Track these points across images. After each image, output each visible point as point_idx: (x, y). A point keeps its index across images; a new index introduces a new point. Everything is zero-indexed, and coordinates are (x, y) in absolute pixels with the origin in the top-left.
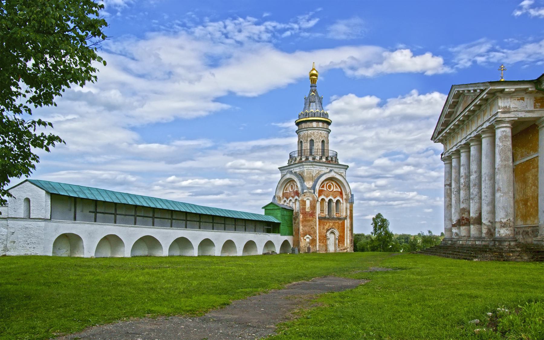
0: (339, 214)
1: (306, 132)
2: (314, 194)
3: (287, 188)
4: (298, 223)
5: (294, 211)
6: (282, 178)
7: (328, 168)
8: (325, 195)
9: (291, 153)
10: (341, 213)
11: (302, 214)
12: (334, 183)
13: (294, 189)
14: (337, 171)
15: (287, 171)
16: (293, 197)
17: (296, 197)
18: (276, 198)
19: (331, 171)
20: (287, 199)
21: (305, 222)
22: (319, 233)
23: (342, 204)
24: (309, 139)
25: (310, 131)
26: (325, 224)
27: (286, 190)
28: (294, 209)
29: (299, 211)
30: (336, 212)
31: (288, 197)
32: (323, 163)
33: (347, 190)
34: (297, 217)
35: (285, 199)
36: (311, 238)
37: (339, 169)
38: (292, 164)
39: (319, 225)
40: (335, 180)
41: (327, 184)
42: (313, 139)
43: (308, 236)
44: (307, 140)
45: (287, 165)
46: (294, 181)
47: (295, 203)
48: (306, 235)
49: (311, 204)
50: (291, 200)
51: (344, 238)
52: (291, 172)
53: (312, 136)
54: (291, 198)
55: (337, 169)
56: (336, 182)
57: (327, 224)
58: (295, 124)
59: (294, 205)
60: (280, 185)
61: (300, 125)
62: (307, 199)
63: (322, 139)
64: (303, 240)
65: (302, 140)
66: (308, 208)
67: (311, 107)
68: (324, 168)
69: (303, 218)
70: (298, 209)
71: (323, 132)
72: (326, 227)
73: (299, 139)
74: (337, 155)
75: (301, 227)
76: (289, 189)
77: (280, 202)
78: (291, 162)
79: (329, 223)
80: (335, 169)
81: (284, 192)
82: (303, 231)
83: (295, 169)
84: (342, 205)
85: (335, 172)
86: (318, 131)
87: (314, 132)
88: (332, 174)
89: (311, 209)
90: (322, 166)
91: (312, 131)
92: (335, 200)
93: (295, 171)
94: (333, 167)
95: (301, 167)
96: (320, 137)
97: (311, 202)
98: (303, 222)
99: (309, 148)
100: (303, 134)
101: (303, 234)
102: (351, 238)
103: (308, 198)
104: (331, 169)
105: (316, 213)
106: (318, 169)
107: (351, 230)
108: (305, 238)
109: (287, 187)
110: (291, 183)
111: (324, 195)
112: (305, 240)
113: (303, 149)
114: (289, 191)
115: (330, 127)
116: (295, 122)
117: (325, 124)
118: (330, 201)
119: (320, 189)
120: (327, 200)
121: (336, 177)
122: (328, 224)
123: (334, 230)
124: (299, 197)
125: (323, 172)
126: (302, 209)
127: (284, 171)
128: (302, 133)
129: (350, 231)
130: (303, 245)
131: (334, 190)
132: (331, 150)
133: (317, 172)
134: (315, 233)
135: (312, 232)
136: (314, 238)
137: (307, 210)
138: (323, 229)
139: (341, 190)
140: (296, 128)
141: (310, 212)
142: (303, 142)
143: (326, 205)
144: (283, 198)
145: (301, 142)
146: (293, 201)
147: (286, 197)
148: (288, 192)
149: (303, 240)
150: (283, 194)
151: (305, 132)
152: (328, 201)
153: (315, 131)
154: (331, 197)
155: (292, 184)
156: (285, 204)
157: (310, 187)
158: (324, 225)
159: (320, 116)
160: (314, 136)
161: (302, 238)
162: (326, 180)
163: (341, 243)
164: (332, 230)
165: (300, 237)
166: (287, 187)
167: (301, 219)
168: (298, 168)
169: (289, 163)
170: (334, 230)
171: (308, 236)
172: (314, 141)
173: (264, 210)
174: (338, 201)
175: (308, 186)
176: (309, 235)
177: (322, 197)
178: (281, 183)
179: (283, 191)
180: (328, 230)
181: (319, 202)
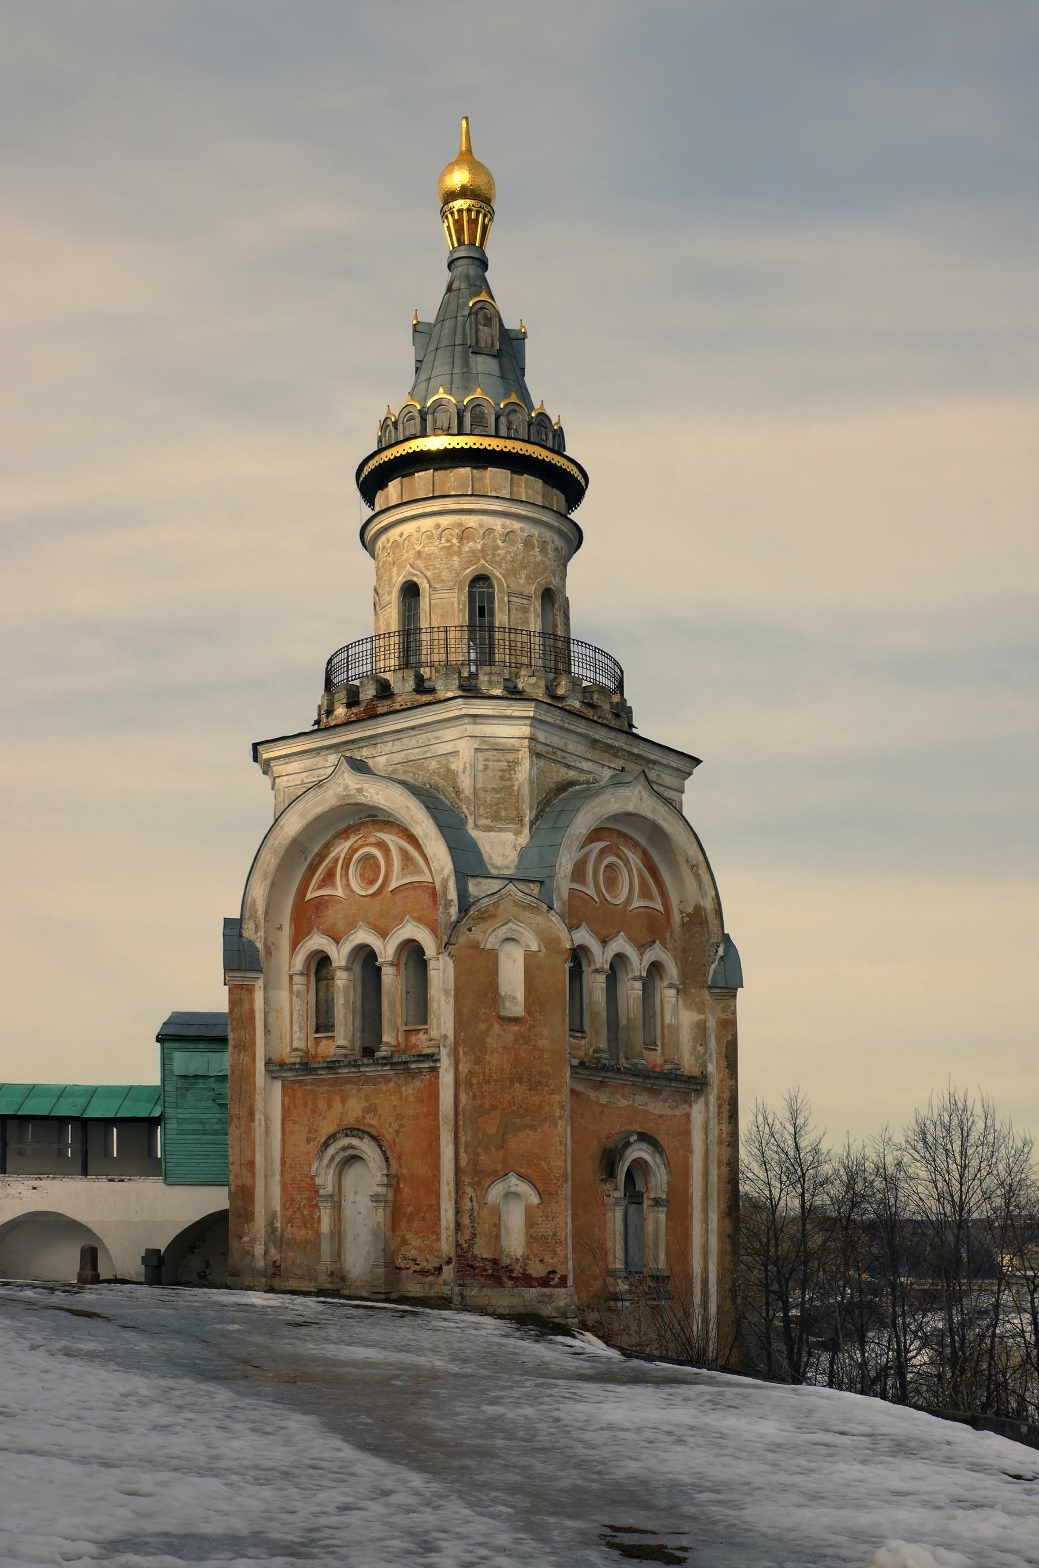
12: (390, 839)
26: (322, 1105)
41: (353, 850)
51: (438, 1195)
57: (330, 1106)
63: (399, 580)
79: (343, 1101)
120: (339, 956)
121: (361, 799)
122: (337, 1104)
131: (393, 885)
138: (309, 1141)
154: (363, 936)
158: (314, 1111)
163: (416, 1224)
164: (346, 1141)
177: (317, 942)
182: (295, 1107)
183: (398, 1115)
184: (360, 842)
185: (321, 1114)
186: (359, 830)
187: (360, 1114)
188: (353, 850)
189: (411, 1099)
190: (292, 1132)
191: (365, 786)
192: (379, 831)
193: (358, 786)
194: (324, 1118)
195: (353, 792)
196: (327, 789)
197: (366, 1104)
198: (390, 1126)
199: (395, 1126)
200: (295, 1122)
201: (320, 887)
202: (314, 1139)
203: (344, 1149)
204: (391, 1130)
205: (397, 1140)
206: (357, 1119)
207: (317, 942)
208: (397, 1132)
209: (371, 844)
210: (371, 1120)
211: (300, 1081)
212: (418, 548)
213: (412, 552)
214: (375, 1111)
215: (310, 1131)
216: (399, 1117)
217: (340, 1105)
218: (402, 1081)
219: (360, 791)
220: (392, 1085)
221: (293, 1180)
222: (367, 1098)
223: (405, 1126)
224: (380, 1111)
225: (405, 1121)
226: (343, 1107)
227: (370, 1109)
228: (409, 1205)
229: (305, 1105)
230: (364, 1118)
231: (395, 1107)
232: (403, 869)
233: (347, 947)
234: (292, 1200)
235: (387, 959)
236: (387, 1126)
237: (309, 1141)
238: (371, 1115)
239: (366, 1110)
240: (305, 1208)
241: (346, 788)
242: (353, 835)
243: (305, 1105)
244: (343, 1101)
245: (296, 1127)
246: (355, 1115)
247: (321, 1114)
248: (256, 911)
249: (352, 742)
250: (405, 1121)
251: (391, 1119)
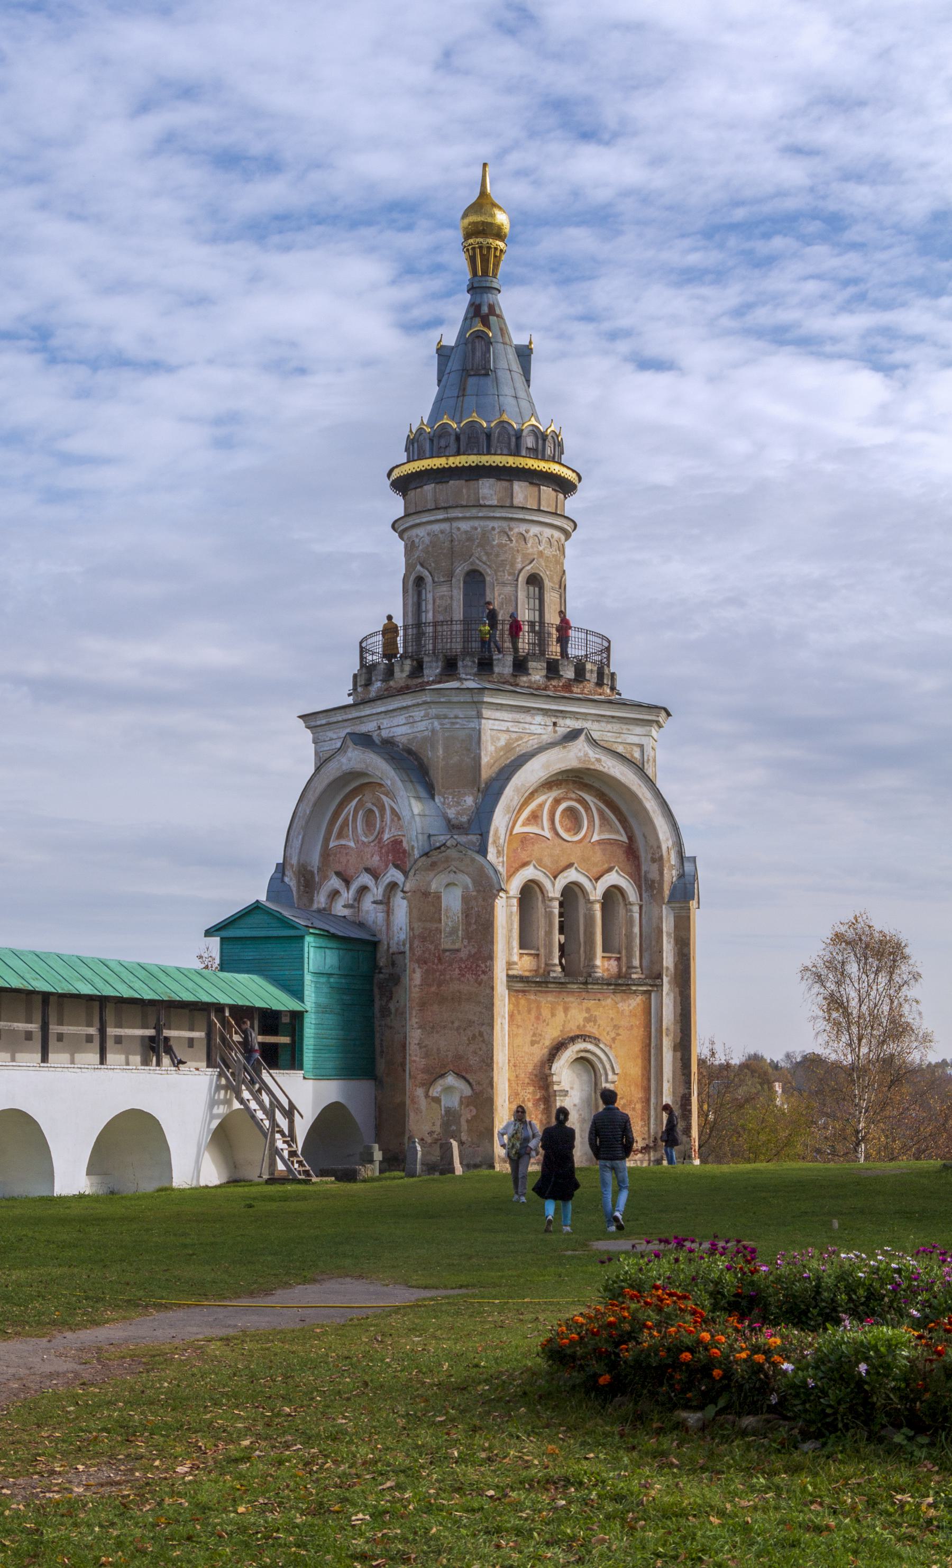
0: (618, 959)
1: (445, 526)
2: (479, 858)
3: (345, 823)
4: (401, 1013)
5: (383, 948)
6: (318, 769)
7: (561, 722)
8: (547, 861)
9: (365, 639)
10: (630, 957)
11: (422, 961)
12: (588, 798)
13: (382, 831)
14: (609, 737)
15: (343, 733)
16: (376, 875)
17: (394, 875)
18: (286, 879)
19: (573, 735)
20: (347, 882)
21: (436, 1007)
22: (514, 1065)
23: (636, 909)
24: (460, 570)
25: (465, 526)
26: (546, 1013)
27: (340, 835)
28: (383, 937)
29: (408, 945)
30: (604, 951)
31: (351, 871)
32: (535, 692)
33: (662, 836)
34: (395, 979)
35: (335, 882)
36: (468, 1091)
37: (616, 727)
38: (373, 694)
39: (511, 1016)
40: (596, 785)
41: (557, 802)
42: (482, 568)
43: (451, 1080)
44: (451, 575)
45: (350, 700)
46: (381, 785)
47: (386, 902)
48: (442, 1076)
49: (467, 913)
50: (364, 889)
52: (365, 741)
53: (478, 552)
54: (366, 879)
55: (609, 727)
56: (601, 796)
57: (553, 1015)
58: (389, 482)
59: (381, 916)
60: (307, 808)
61: (411, 494)
62: (448, 885)
64: (423, 1103)
65: (426, 573)
66: (454, 931)
67: (470, 401)
68: (539, 719)
69: (425, 982)
70: (403, 936)
71: (535, 530)
72: (551, 1034)
73: (409, 567)
74: (608, 649)
75: (415, 1036)
76: (355, 828)
77: (311, 901)
78: (368, 683)
79: (566, 1010)
80: (596, 726)
81: (332, 845)
82: (427, 1055)
83: (385, 723)
84: (637, 916)
85: (593, 743)
86: (504, 524)
87: (484, 534)
88: (581, 754)
89: (468, 936)
90: (527, 710)
91: (476, 523)
92: (596, 892)
93: (385, 734)
94: (585, 716)
95: (418, 714)
96: (519, 560)
97: (466, 899)
98: (423, 1005)
99: (458, 614)
100: (427, 540)
101: (426, 1070)
102: (681, 1091)
103: (451, 877)
104: (577, 725)
105: (490, 957)
106: (504, 726)
107: (684, 1045)
108: (436, 1090)
109: (346, 819)
110: (368, 797)
111: (540, 864)
112: (437, 1100)
113: (430, 617)
114: (357, 841)
115: (571, 505)
116: (389, 475)
117: (547, 492)
118: (571, 893)
119: (518, 829)
120: (554, 890)
123: (590, 1047)
124: (406, 874)
125: (533, 743)
126: (423, 939)
127: (331, 734)
128: (421, 532)
129: (675, 1049)
130: (426, 1128)
132: (579, 630)
133: (502, 743)
134: (488, 1062)
135: (474, 1061)
136: (482, 1092)
137: (446, 943)
138: (533, 1043)
139: (631, 838)
140: (396, 506)
141: (463, 954)
142: (429, 579)
143: (549, 915)
144: (325, 878)
145: (420, 581)
146: (377, 892)
147: (338, 874)
148: (352, 844)
149: (423, 1103)
150: (326, 854)
151: (436, 527)
152: (557, 894)
153: (491, 524)
154: (572, 875)
155: (369, 805)
156: (339, 909)
157: (464, 819)
158: (538, 1018)
159: (518, 446)
160: (487, 554)
161: (420, 1092)
162: (549, 784)
165: (409, 1083)
166: (346, 819)
167: (415, 993)
168: (401, 719)
169: (355, 689)
170: (590, 1047)
171: (451, 1080)
172: (488, 579)
173: (217, 940)
174: (612, 896)
175: (451, 813)
176: (459, 1075)
178: (312, 797)
179: (327, 840)
180: (557, 1048)
181: (515, 902)
182: (519, 1012)
183: (615, 1026)
184: (562, 796)
185: (545, 1021)
186: (561, 784)
187: (582, 1023)
188: (557, 802)
189: (627, 1013)
190: (517, 1035)
191: (603, 758)
192: (579, 790)
193: (597, 756)
194: (548, 1025)
195: (593, 760)
196: (569, 751)
197: (587, 1015)
198: (608, 1034)
199: (613, 1035)
200: (518, 1026)
201: (524, 825)
202: (538, 1042)
203: (578, 1052)
204: (608, 1038)
205: (613, 1046)
206: (578, 1027)
207: (529, 873)
208: (614, 1039)
209: (571, 799)
210: (591, 1029)
211: (524, 991)
212: (541, 548)
213: (535, 549)
214: (595, 1021)
215: (534, 1035)
216: (616, 1027)
217: (562, 1014)
218: (618, 997)
219: (599, 760)
220: (609, 1001)
221: (517, 1077)
222: (588, 1010)
223: (618, 1035)
224: (599, 1022)
225: (620, 1031)
226: (566, 1016)
227: (591, 1019)
228: (622, 1098)
229: (529, 1011)
230: (584, 1026)
231: (612, 1019)
232: (601, 826)
233: (561, 882)
234: (517, 1094)
235: (598, 898)
236: (605, 1033)
237: (533, 1043)
238: (592, 1024)
239: (587, 1020)
240: (529, 1101)
241: (586, 755)
242: (555, 788)
243: (529, 1011)
244: (566, 1010)
245: (521, 1031)
246: (577, 1024)
247: (545, 1021)
248: (499, 838)
249: (562, 711)
250: (620, 1031)
251: (608, 1029)
